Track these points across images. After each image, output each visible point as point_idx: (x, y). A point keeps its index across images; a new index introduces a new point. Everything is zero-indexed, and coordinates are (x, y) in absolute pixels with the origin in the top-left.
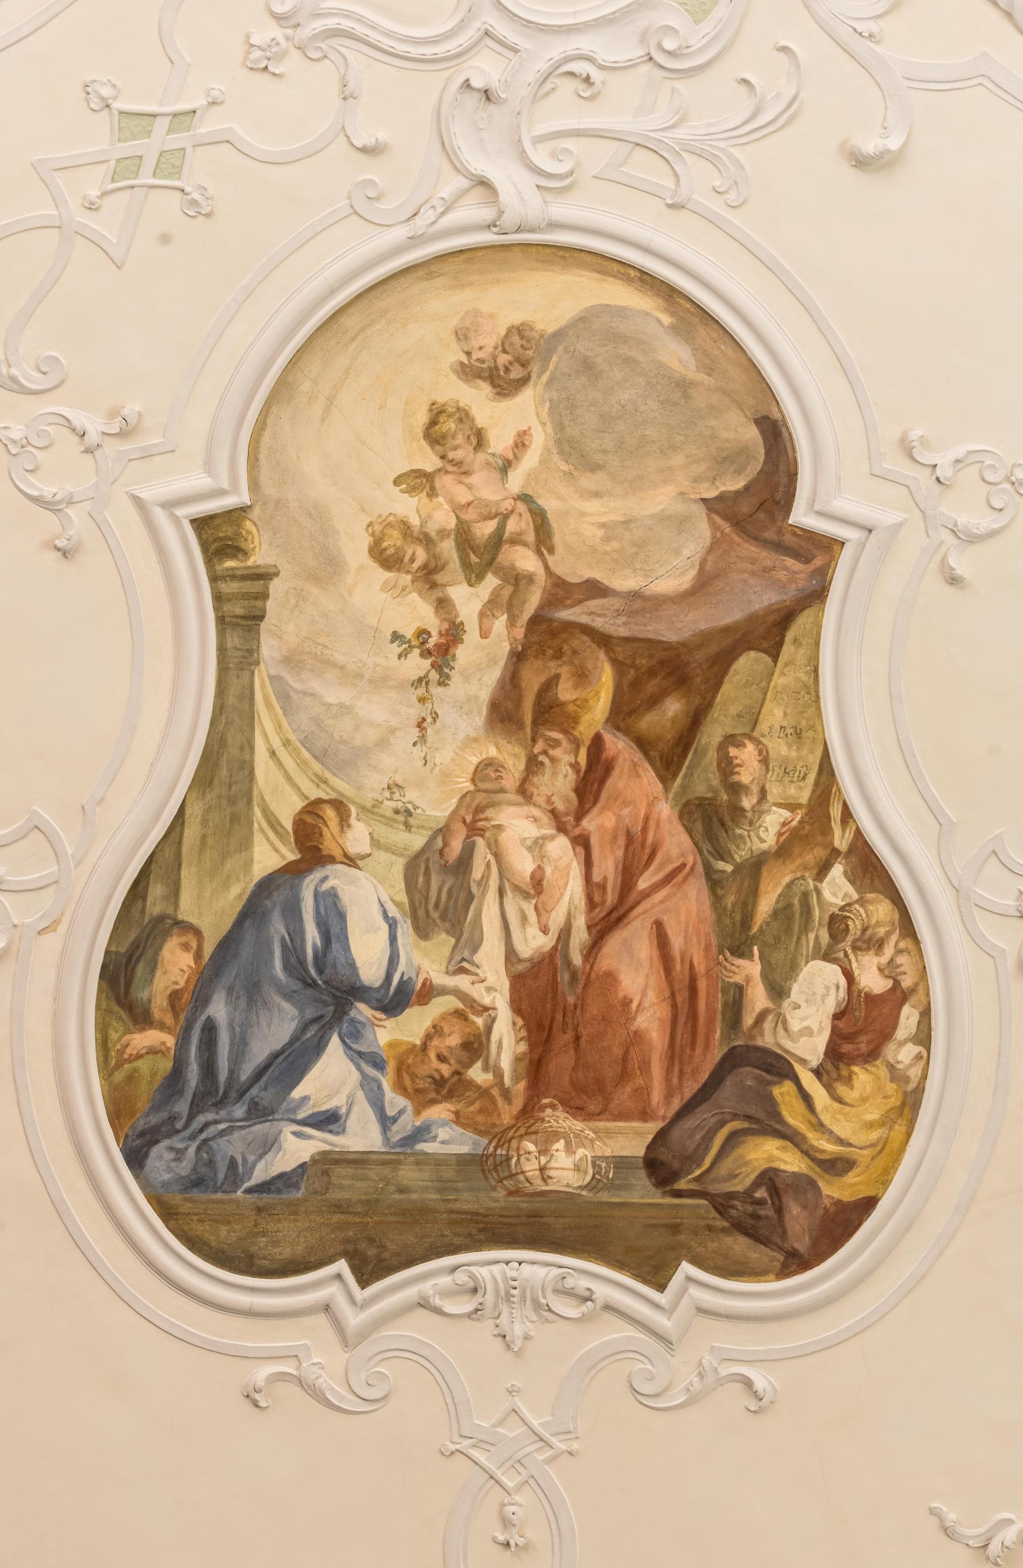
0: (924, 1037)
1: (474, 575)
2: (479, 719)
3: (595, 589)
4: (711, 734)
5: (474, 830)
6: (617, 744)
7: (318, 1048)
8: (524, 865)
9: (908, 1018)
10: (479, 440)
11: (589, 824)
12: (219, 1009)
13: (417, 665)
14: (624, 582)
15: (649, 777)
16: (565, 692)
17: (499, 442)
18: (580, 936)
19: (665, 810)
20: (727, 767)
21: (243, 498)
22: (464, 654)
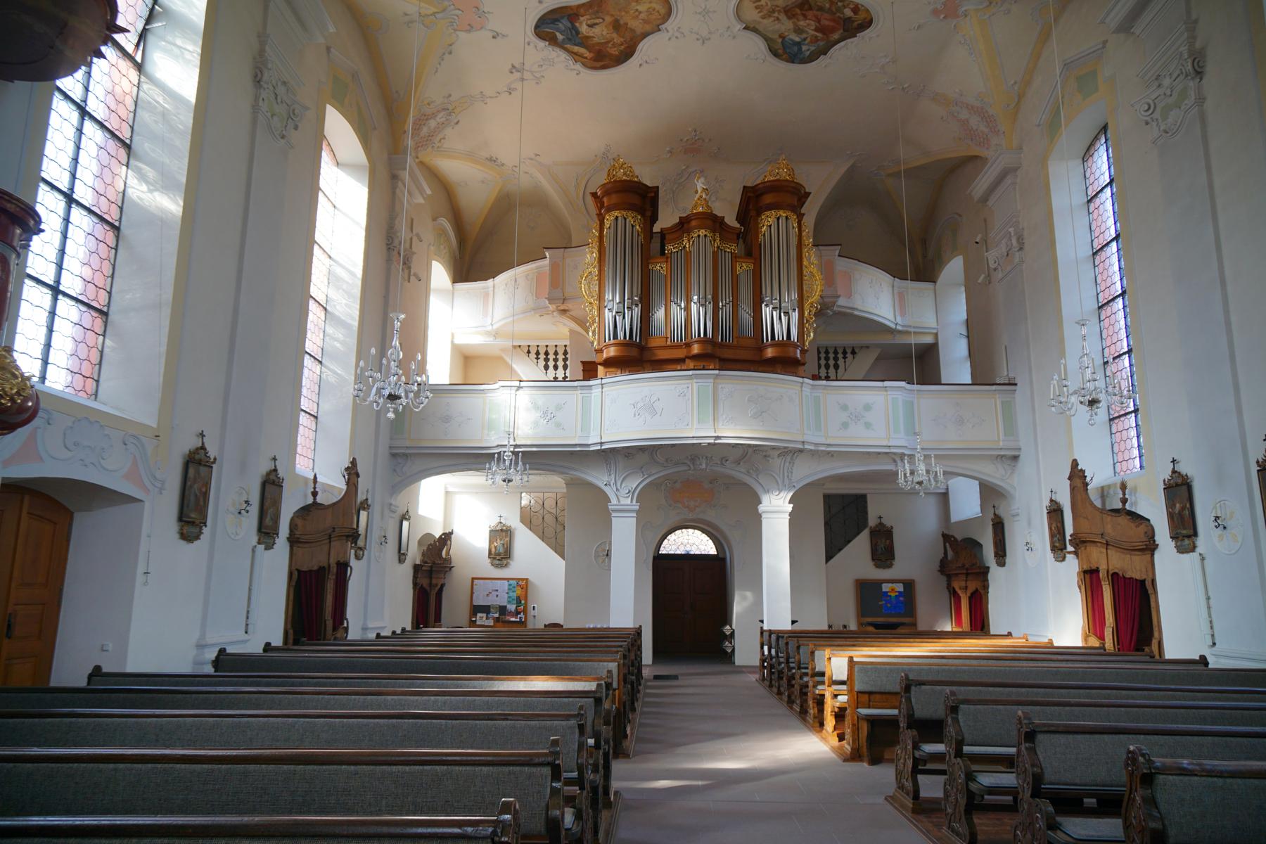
0: (863, 6)
1: (774, 13)
2: (788, 21)
3: (787, 6)
4: (813, 4)
5: (797, 26)
6: (804, 12)
7: (801, 48)
8: (805, 24)
9: (860, 6)
10: (762, 5)
11: (808, 17)
12: (788, 51)
13: (776, 22)
14: (790, 3)
15: (811, 12)
16: (794, 13)
17: (764, 4)
18: (818, 25)
19: (815, 12)
20: (818, 6)
21: (744, 25)
22: (780, 17)
